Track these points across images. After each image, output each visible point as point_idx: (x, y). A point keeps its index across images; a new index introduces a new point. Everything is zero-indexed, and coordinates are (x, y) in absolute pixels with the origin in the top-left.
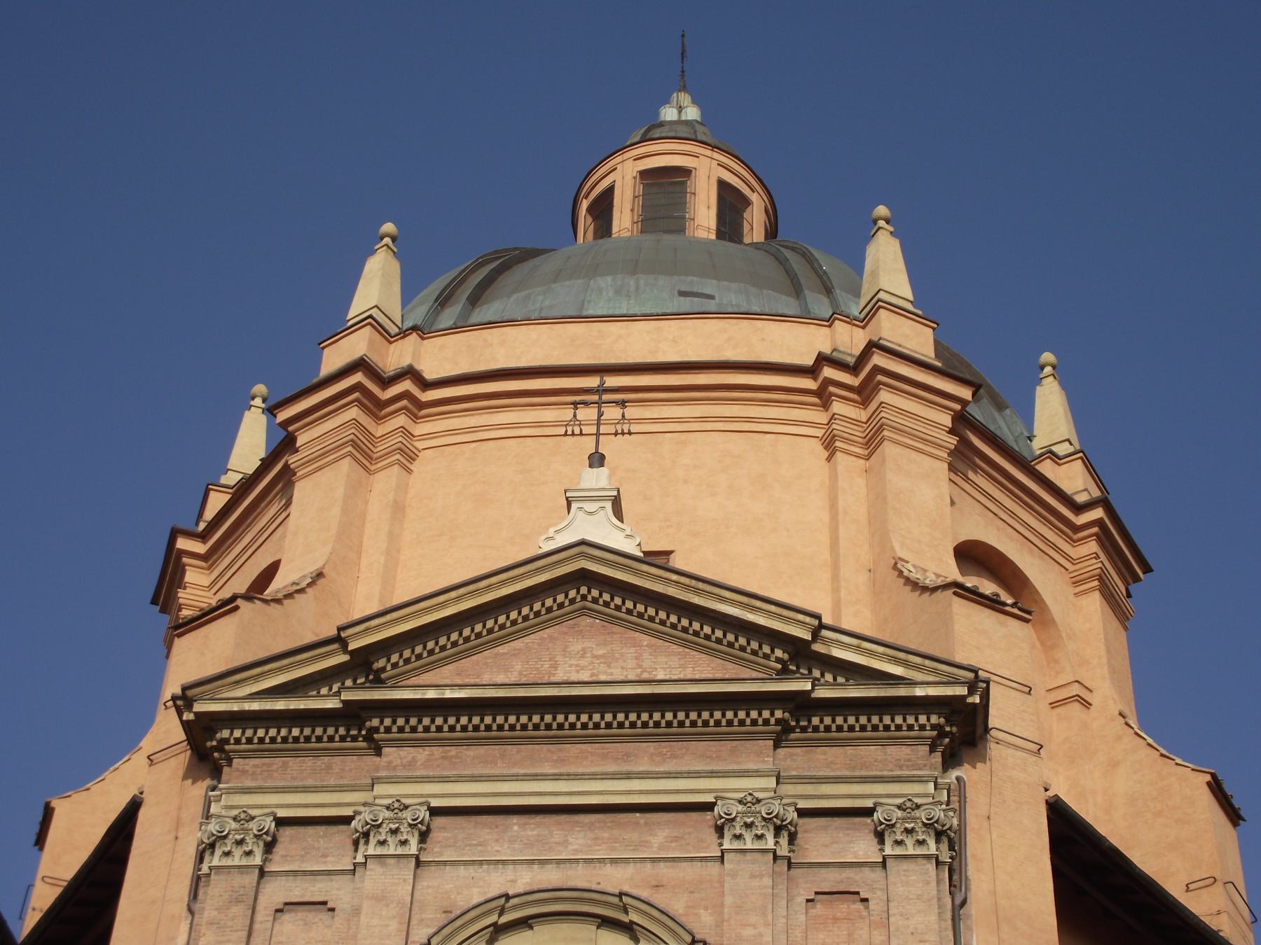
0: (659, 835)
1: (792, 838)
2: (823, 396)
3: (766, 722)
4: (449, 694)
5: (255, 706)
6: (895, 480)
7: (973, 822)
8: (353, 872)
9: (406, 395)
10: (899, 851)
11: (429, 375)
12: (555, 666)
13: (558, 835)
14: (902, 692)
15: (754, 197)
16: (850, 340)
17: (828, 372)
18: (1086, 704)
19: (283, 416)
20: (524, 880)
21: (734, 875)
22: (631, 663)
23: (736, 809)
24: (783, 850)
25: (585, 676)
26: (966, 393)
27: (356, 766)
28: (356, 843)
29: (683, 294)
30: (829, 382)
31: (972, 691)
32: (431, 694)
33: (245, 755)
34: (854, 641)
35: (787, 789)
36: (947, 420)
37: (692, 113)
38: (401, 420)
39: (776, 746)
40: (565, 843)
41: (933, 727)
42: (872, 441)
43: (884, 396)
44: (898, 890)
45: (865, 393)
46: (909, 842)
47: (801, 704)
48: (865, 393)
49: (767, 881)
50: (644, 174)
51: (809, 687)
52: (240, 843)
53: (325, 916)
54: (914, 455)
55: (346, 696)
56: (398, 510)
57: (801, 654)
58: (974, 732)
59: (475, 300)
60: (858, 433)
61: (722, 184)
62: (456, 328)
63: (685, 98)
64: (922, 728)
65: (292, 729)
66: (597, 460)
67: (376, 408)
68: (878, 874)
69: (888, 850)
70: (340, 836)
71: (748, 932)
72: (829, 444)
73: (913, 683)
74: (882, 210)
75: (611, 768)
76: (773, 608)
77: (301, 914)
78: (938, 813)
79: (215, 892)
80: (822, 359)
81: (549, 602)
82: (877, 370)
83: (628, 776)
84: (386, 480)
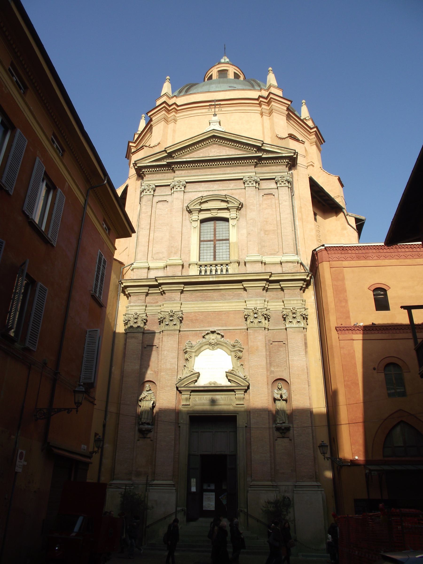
0: (232, 185)
1: (259, 184)
2: (260, 104)
3: (253, 162)
4: (188, 160)
5: (149, 164)
9: (174, 108)
10: (280, 185)
11: (179, 104)
13: (212, 186)
15: (241, 76)
16: (265, 94)
17: (261, 99)
18: (313, 166)
19: (149, 115)
20: (205, 194)
21: (248, 191)
23: (247, 179)
24: (257, 186)
26: (289, 103)
27: (170, 175)
28: (171, 189)
29: (230, 87)
30: (261, 101)
31: (294, 155)
32: (185, 160)
33: (148, 174)
35: (258, 175)
36: (286, 109)
37: (227, 60)
38: (174, 113)
39: (255, 167)
40: (213, 187)
41: (287, 162)
42: (270, 113)
43: (273, 103)
44: (280, 192)
45: (269, 103)
46: (282, 184)
47: (260, 159)
48: (269, 103)
49: (254, 192)
50: (219, 71)
51: (261, 155)
52: (148, 190)
53: (166, 203)
54: (279, 115)
55: (168, 161)
56: (174, 131)
57: (259, 149)
58: (294, 164)
59: (186, 92)
60: (268, 112)
61: (235, 73)
62: (184, 95)
63: (226, 58)
64: (284, 162)
65: (156, 168)
66: (215, 115)
67: (168, 111)
68: (277, 190)
69: (278, 185)
70: (168, 188)
71: (251, 201)
72: (262, 114)
74: (270, 69)
75: (222, 173)
78: (288, 178)
79: (144, 200)
80: (260, 97)
81: (207, 142)
82: (271, 98)
83: (225, 174)
84: (171, 125)
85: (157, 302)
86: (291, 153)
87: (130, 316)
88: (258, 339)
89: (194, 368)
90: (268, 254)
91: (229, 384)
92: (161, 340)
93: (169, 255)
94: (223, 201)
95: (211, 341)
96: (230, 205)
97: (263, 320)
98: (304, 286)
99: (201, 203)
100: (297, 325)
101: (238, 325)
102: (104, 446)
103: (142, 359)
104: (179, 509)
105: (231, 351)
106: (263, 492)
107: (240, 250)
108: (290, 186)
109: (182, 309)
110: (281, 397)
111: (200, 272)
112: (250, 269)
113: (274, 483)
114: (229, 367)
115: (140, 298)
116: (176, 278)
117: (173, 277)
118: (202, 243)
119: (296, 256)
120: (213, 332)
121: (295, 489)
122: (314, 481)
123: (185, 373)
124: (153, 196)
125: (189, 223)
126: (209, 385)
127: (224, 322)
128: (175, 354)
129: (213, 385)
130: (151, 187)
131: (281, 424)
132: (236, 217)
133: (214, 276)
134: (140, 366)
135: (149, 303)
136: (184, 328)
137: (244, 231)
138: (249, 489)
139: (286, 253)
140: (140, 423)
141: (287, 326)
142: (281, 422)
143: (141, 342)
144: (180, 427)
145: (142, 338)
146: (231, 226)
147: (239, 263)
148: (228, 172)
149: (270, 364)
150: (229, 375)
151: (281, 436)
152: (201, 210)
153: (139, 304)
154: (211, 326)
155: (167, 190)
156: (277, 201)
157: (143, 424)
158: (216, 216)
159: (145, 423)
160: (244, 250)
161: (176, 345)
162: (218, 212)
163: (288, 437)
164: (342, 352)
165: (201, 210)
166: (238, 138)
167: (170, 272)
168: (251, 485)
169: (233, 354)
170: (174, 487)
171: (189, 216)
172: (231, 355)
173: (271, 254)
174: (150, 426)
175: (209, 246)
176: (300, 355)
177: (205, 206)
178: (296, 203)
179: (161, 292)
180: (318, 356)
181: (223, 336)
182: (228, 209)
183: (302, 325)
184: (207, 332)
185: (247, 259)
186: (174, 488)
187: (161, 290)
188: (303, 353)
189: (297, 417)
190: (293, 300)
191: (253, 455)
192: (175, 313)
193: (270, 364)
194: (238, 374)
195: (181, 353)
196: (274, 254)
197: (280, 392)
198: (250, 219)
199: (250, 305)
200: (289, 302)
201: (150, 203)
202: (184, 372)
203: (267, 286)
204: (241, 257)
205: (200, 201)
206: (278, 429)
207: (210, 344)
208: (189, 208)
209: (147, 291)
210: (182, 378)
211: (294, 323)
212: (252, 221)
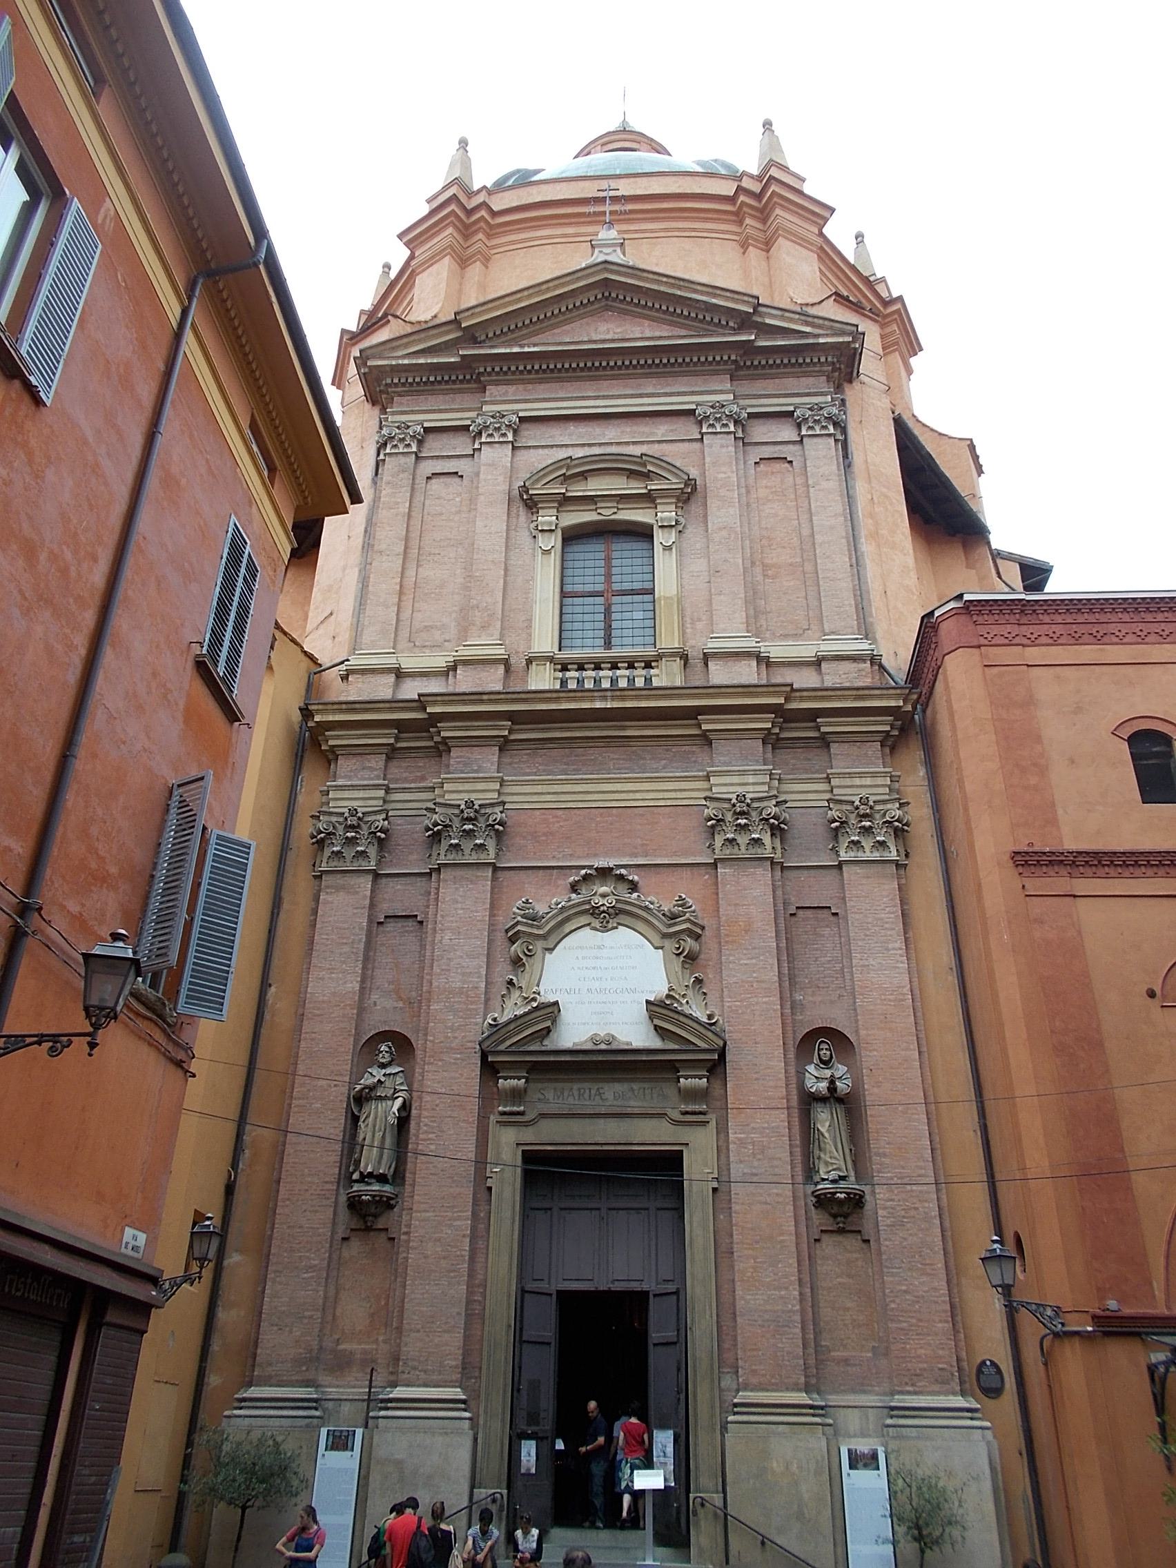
0: (661, 430)
3: (726, 362)
5: (406, 362)
7: (850, 420)
11: (495, 208)
13: (598, 430)
14: (811, 341)
17: (742, 198)
20: (579, 453)
24: (740, 434)
34: (779, 313)
35: (742, 402)
53: (457, 480)
57: (745, 322)
58: (852, 372)
68: (797, 447)
71: (723, 475)
73: (818, 336)
76: (728, 294)
77: (443, 479)
78: (835, 411)
83: (641, 396)
86: (843, 333)
87: (334, 819)
88: (750, 896)
90: (774, 637)
91: (657, 1043)
92: (432, 896)
93: (464, 632)
94: (632, 474)
95: (598, 901)
97: (767, 839)
98: (896, 733)
99: (566, 479)
100: (876, 855)
101: (685, 853)
102: (226, 1263)
103: (366, 959)
104: (481, 1493)
105: (665, 936)
106: (781, 1427)
107: (688, 619)
109: (503, 798)
110: (832, 1088)
111: (564, 682)
112: (719, 674)
113: (815, 1396)
114: (659, 988)
115: (368, 765)
116: (485, 697)
117: (477, 697)
118: (568, 601)
120: (604, 873)
122: (954, 1394)
123: (514, 1008)
124: (417, 458)
125: (530, 540)
126: (589, 1046)
127: (639, 841)
128: (481, 943)
129: (603, 1047)
130: (410, 431)
131: (834, 1181)
132: (677, 521)
133: (609, 694)
134: (363, 981)
135: (396, 781)
136: (509, 861)
137: (698, 565)
138: (731, 1418)
139: (833, 633)
140: (356, 1176)
141: (844, 856)
142: (833, 1175)
143: (367, 902)
144: (490, 1189)
145: (372, 891)
146: (658, 548)
147: (685, 658)
148: (650, 390)
149: (790, 980)
150: (656, 1009)
151: (834, 1228)
152: (564, 501)
153: (365, 782)
154: (596, 855)
155: (461, 445)
156: (799, 481)
157: (363, 1178)
158: (613, 517)
159: (370, 1175)
160: (699, 620)
161: (483, 914)
163: (859, 1232)
166: (679, 288)
167: (465, 681)
168: (736, 1405)
169: (668, 943)
170: (465, 1410)
171: (527, 518)
172: (662, 948)
173: (785, 636)
174: (387, 1188)
176: (888, 950)
177: (577, 490)
178: (861, 489)
179: (436, 747)
180: (945, 959)
181: (634, 887)
182: (649, 498)
183: (893, 855)
184: (583, 872)
185: (713, 645)
186: (467, 1415)
187: (437, 739)
188: (899, 943)
189: (887, 1161)
190: (861, 775)
191: (739, 1292)
192: (483, 811)
193: (792, 978)
194: (688, 1011)
195: (500, 937)
196: (795, 636)
197: (828, 1073)
198: (720, 529)
199: (724, 789)
200: (848, 782)
201: (406, 478)
202: (509, 1004)
203: (777, 730)
204: (691, 642)
206: (823, 1201)
207: (594, 912)
208: (527, 492)
209: (392, 741)
210: (502, 1020)
212: (724, 533)
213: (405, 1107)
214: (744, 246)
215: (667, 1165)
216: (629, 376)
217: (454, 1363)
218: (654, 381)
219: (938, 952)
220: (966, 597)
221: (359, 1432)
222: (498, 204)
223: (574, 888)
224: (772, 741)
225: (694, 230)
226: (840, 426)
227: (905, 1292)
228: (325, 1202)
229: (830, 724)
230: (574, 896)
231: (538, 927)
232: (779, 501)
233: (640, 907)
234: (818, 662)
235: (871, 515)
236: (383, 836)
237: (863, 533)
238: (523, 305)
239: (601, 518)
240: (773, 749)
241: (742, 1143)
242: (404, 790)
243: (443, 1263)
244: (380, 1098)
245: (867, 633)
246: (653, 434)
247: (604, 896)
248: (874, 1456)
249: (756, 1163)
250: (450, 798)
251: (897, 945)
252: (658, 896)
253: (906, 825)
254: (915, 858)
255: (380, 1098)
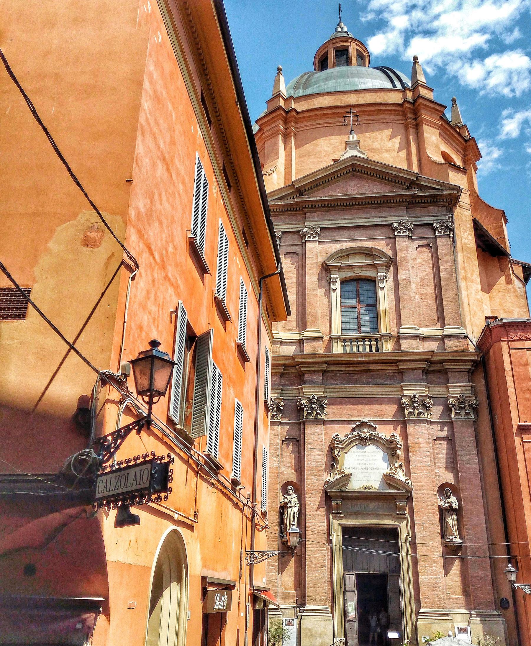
6: (426, 135)
8: (302, 245)
12: (347, 190)
22: (367, 188)
24: (411, 235)
25: (355, 192)
35: (411, 219)
53: (295, 255)
82: (420, 104)
85: (294, 385)
89: (344, 467)
96: (377, 261)
100: (466, 418)
108: (451, 235)
110: (451, 507)
112: (405, 345)
119: (461, 328)
120: (364, 425)
121: (471, 619)
126: (363, 490)
129: (367, 490)
138: (419, 617)
152: (340, 268)
162: (363, 269)
164: (527, 456)
165: (340, 268)
169: (389, 451)
173: (429, 326)
175: (351, 313)
176: (471, 454)
181: (375, 429)
182: (374, 266)
188: (474, 452)
191: (420, 576)
193: (435, 463)
194: (398, 478)
203: (427, 368)
205: (340, 255)
211: (463, 415)
212: (405, 282)
213: (300, 511)
214: (406, 128)
215: (392, 533)
216: (365, 208)
217: (324, 598)
218: (375, 210)
219: (489, 454)
220: (504, 321)
221: (295, 620)
222: (300, 107)
223: (353, 430)
224: (426, 372)
225: (385, 119)
226: (451, 230)
227: (477, 576)
228: (275, 543)
229: (448, 365)
230: (354, 433)
231: (342, 445)
232: (427, 265)
233: (378, 437)
234: (442, 339)
235: (464, 268)
236: (282, 408)
237: (461, 277)
238: (320, 176)
239: (355, 274)
240: (426, 373)
241: (419, 525)
242: (287, 389)
243: (318, 565)
244: (290, 507)
245: (461, 323)
246: (375, 235)
247: (365, 433)
248: (466, 629)
249: (425, 533)
250: (306, 394)
251: (474, 453)
252: (385, 432)
253: (478, 405)
254: (481, 417)
255: (290, 507)
